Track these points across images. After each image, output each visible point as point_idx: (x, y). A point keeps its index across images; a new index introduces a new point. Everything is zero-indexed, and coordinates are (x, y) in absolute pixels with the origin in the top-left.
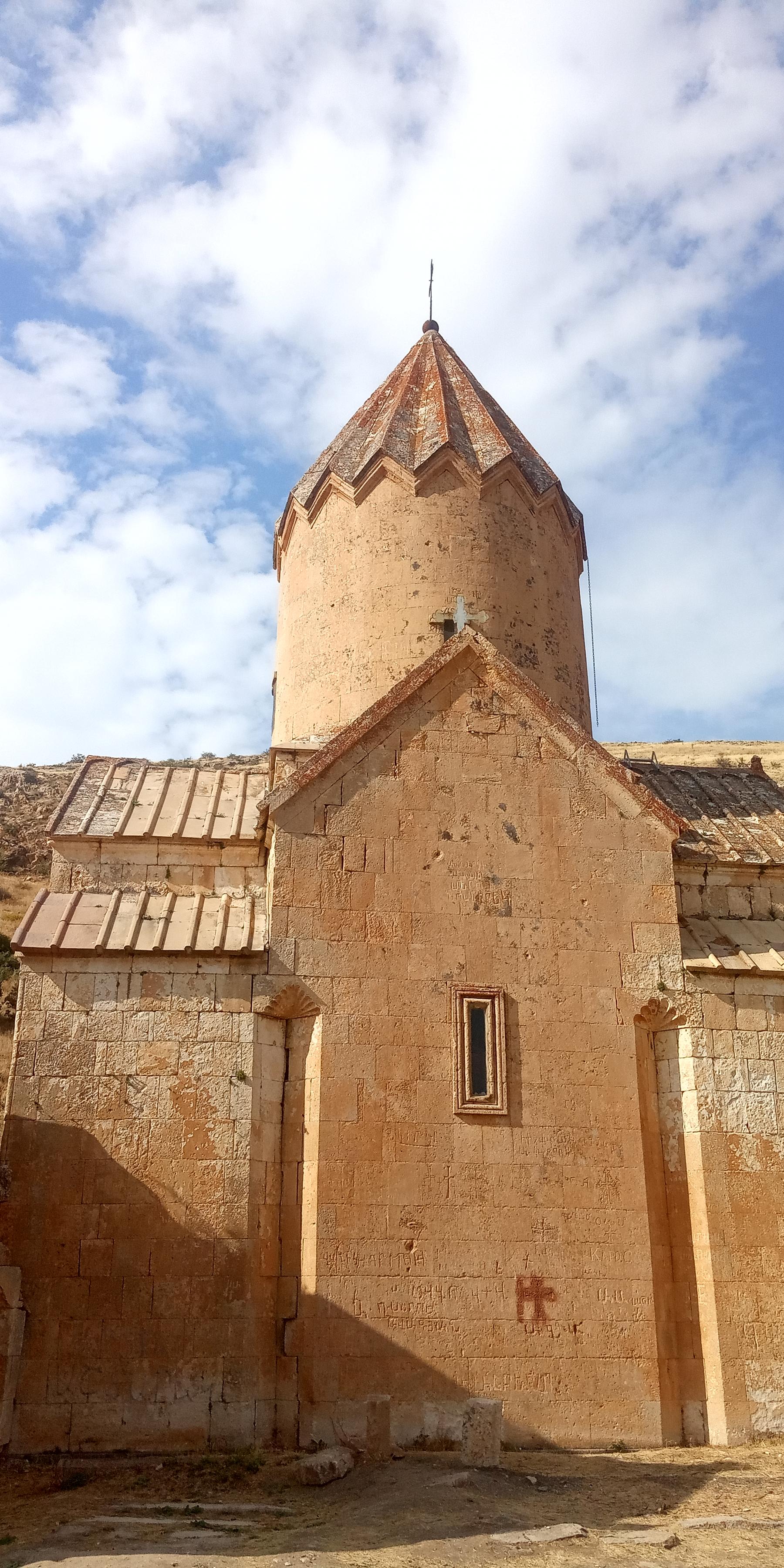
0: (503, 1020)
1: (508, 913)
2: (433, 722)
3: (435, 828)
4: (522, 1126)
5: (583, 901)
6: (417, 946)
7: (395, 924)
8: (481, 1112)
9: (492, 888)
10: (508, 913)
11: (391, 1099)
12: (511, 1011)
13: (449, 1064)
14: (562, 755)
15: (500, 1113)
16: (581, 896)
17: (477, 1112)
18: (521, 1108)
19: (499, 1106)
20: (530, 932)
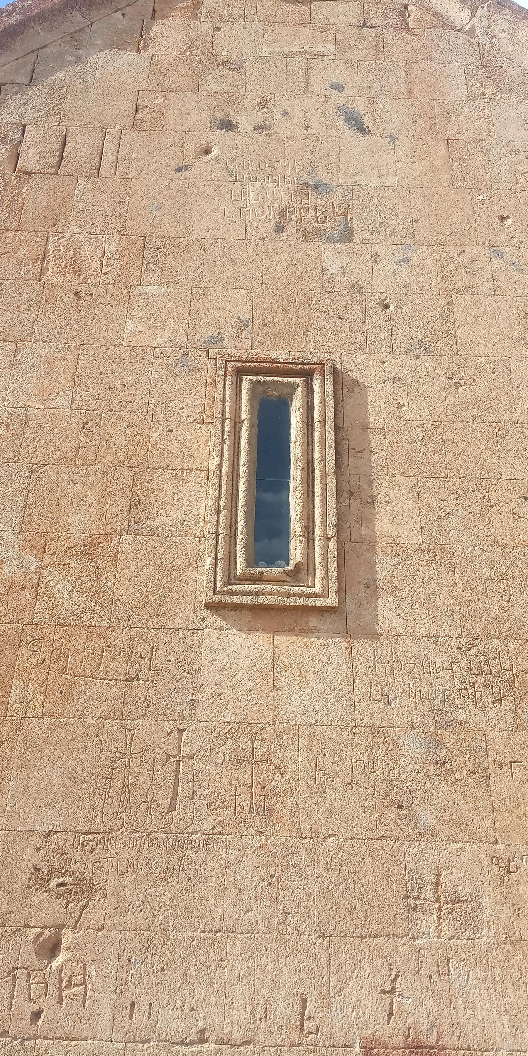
0: (330, 415)
1: (347, 235)
3: (205, 115)
5: (503, 219)
6: (149, 289)
7: (108, 254)
8: (272, 601)
9: (314, 199)
10: (347, 235)
12: (350, 403)
15: (319, 602)
16: (497, 210)
17: (261, 600)
18: (375, 596)
19: (318, 588)
20: (392, 266)
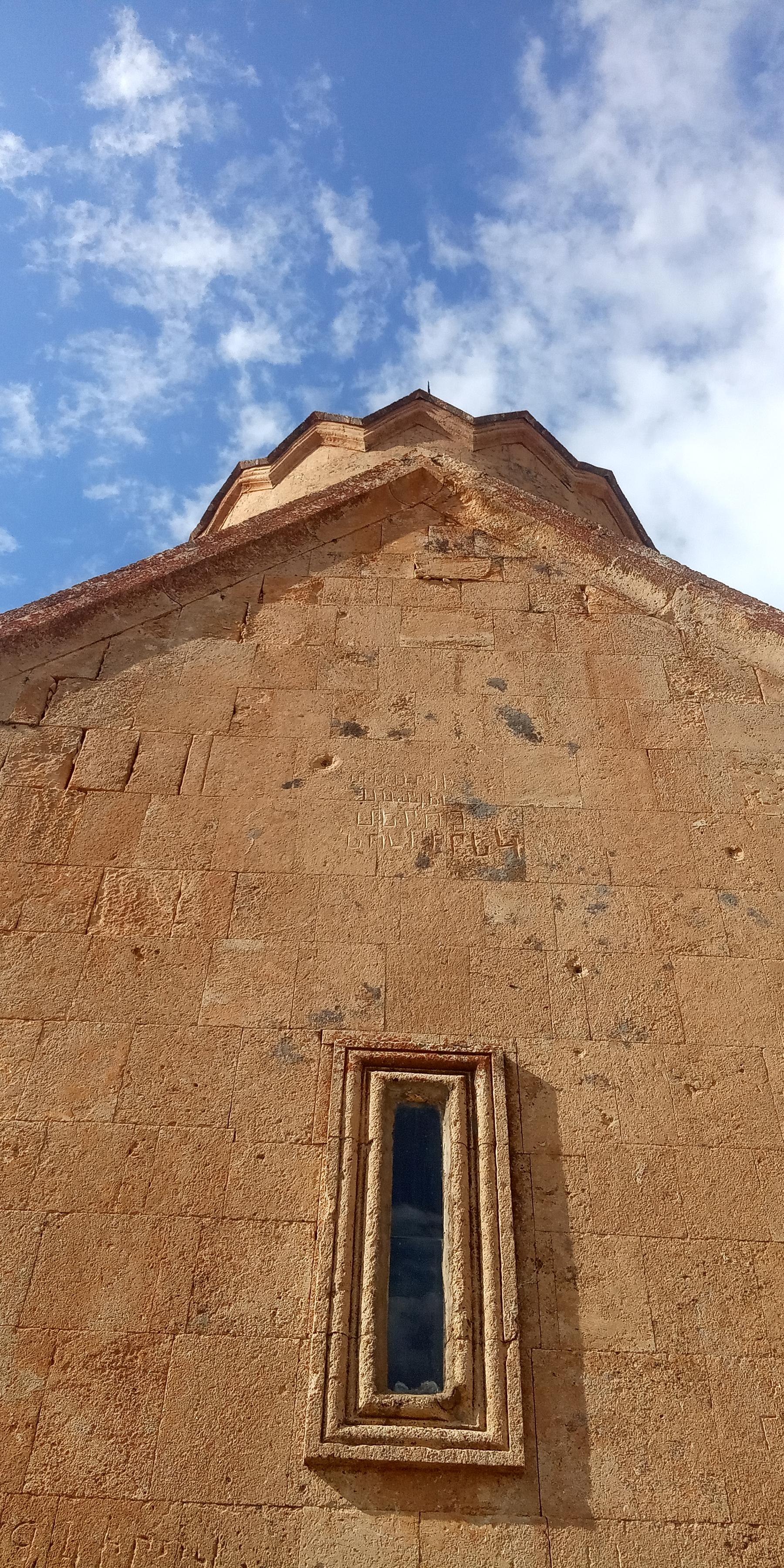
0: (502, 1133)
1: (517, 872)
2: (341, 567)
3: (324, 718)
4: (588, 1521)
5: (731, 852)
6: (240, 944)
7: (185, 895)
8: (415, 1454)
9: (470, 824)
10: (517, 872)
11: (59, 1403)
12: (531, 1114)
13: (301, 1274)
14: (639, 609)
15: (494, 1458)
16: (722, 840)
17: (398, 1453)
18: (584, 1446)
19: (490, 1432)
20: (581, 913)
